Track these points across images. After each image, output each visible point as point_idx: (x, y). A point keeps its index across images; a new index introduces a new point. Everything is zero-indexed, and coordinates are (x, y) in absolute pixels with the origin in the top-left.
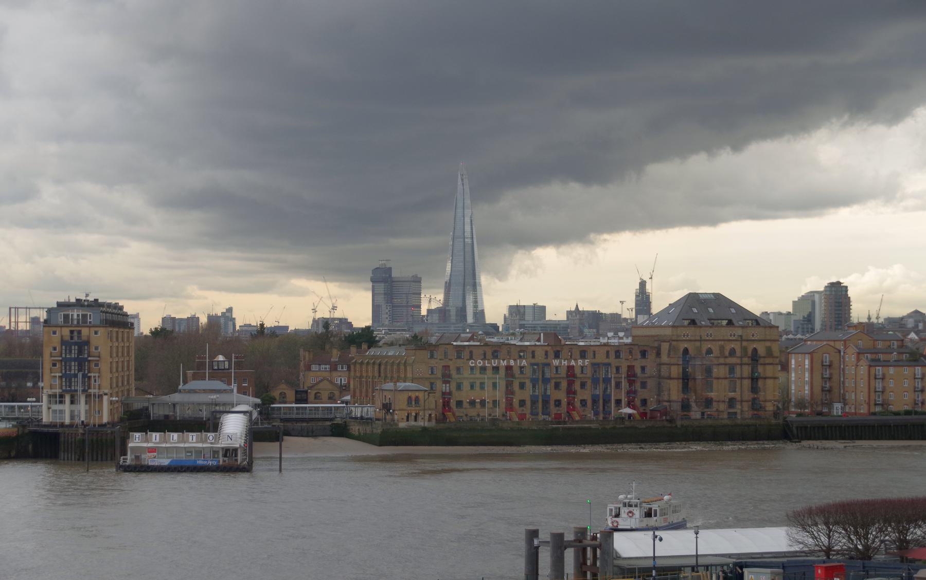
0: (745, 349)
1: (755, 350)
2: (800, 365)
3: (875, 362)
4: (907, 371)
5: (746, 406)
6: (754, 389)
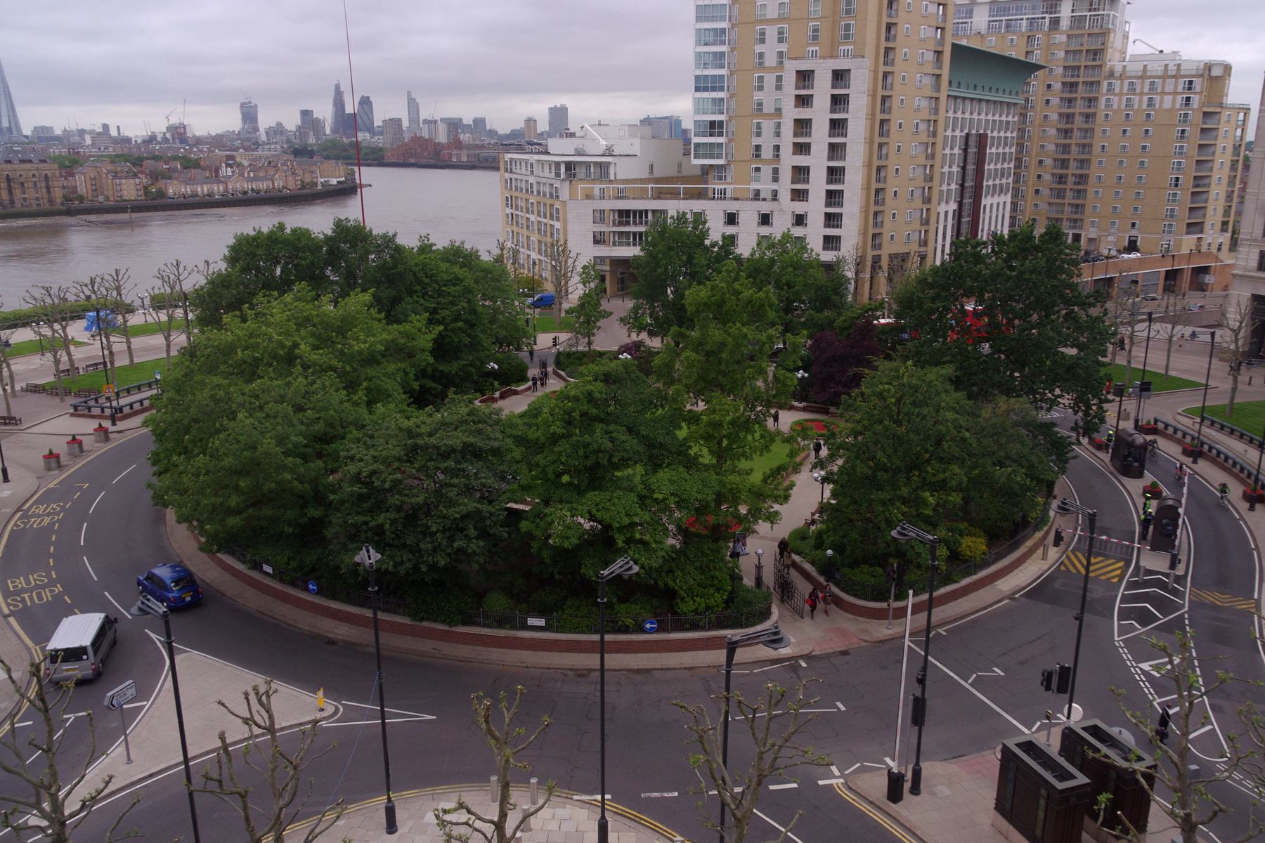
0: (40, 174)
1: (46, 175)
2: (80, 178)
3: (115, 177)
4: (131, 181)
5: (45, 201)
6: (49, 192)
